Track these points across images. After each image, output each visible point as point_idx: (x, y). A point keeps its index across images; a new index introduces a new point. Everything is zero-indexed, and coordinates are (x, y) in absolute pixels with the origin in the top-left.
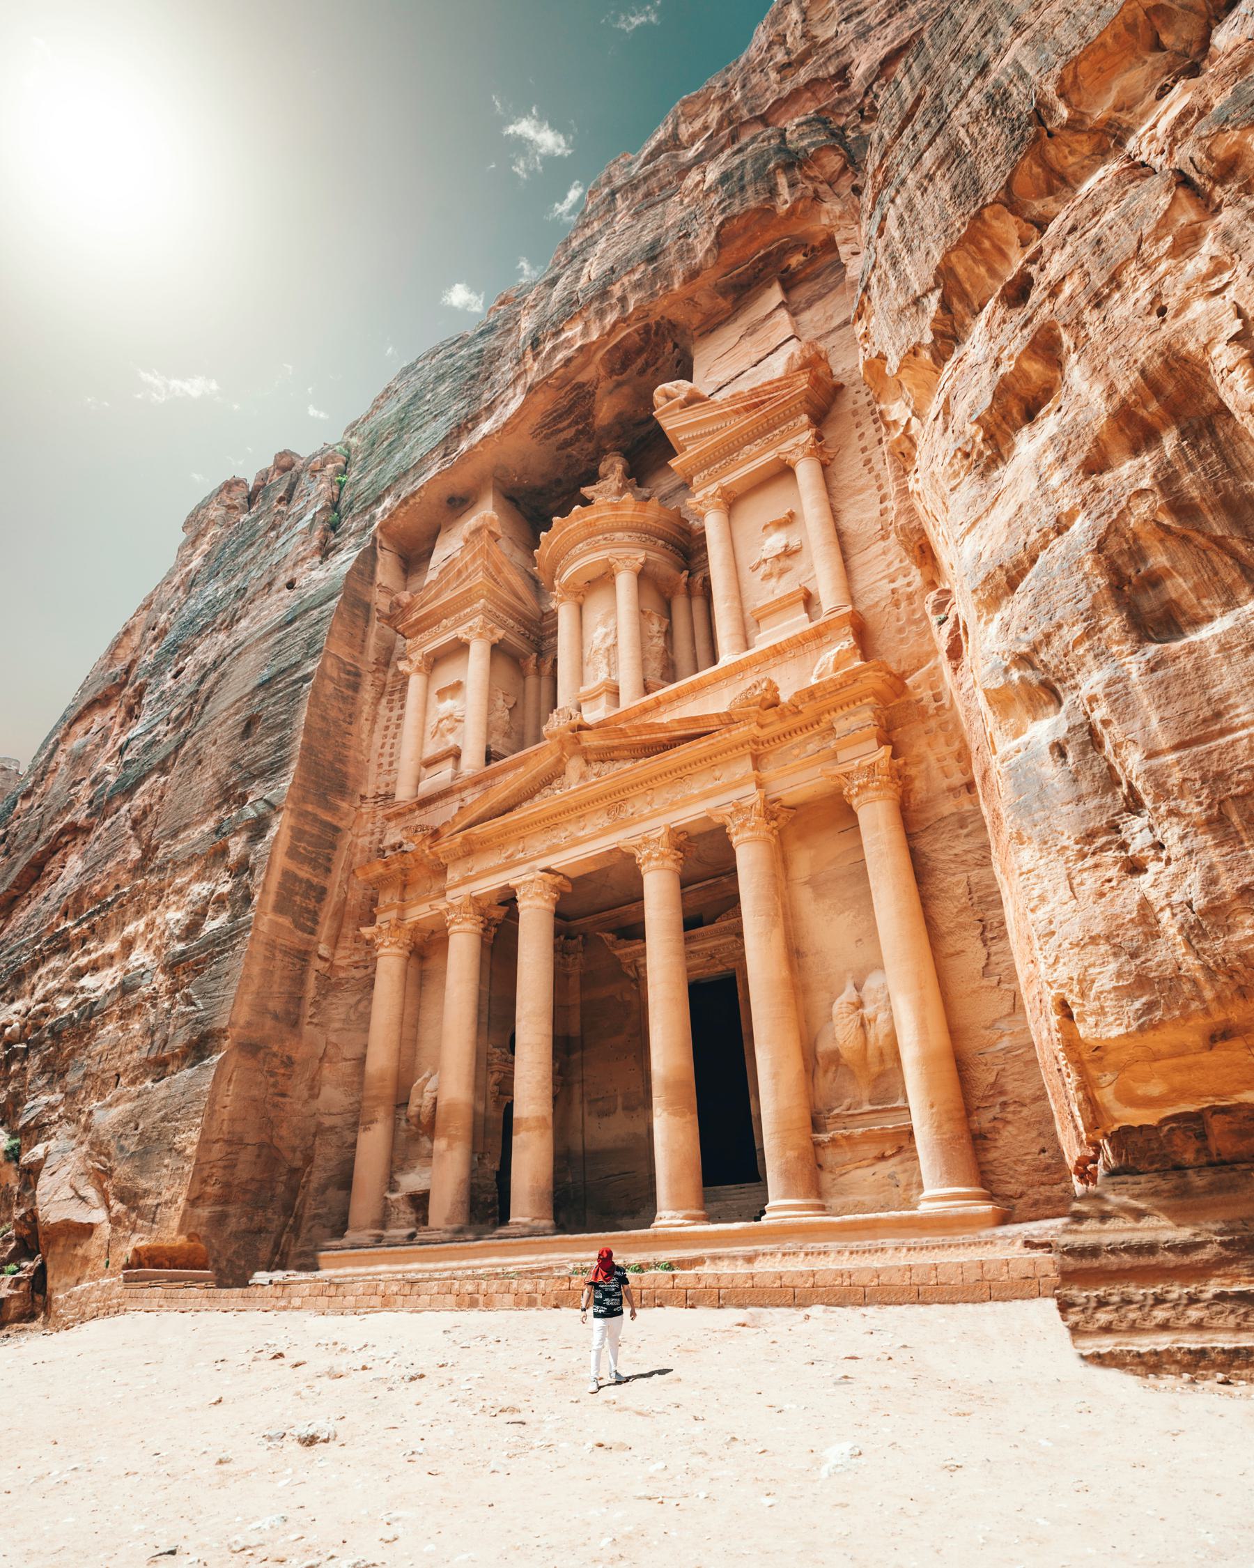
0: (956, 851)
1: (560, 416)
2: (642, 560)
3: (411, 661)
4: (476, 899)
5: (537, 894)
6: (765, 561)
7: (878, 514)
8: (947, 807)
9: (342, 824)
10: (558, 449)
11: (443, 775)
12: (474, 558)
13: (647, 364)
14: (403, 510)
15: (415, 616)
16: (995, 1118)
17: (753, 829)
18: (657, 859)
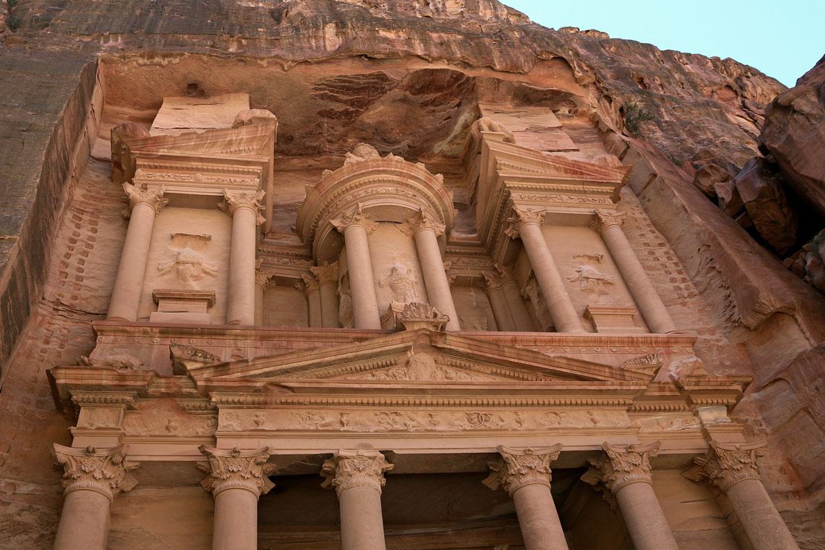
1: (348, 89)
4: (273, 459)
10: (320, 113)
11: (198, 315)
12: (251, 141)
13: (433, 102)
14: (141, 61)
15: (162, 152)
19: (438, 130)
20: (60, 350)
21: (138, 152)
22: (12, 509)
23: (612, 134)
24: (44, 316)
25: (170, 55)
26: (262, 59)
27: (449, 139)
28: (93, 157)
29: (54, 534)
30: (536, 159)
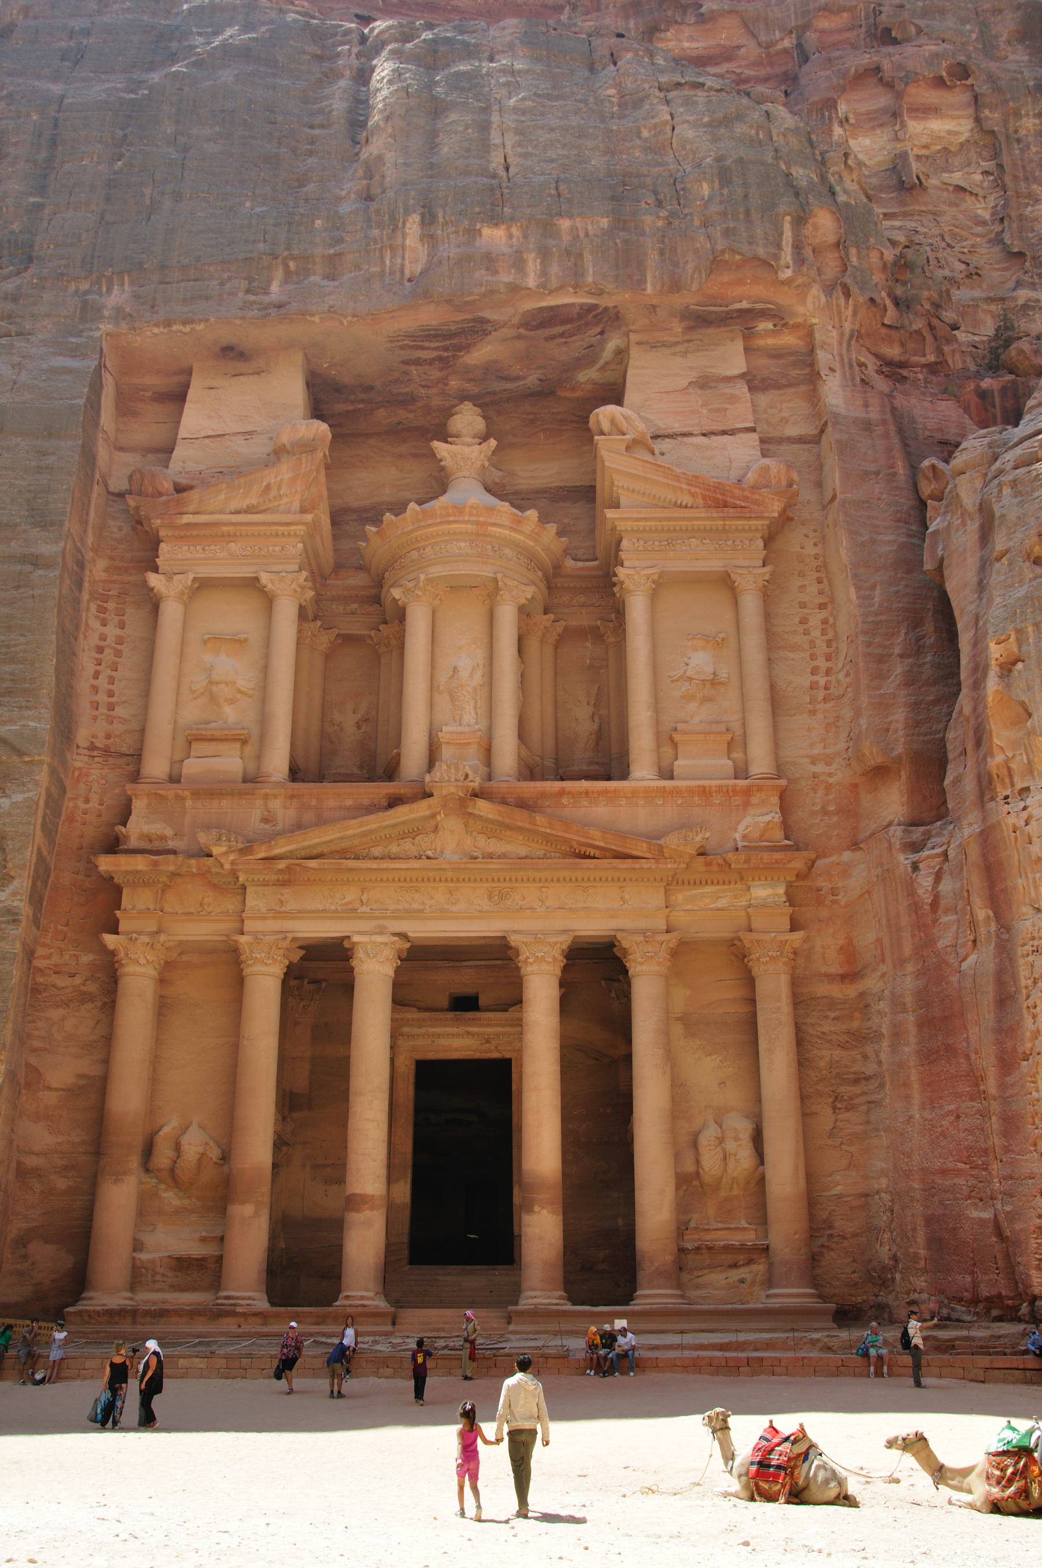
0: (826, 1029)
1: (436, 336)
2: (529, 597)
3: (170, 579)
4: (294, 939)
5: (388, 959)
6: (690, 679)
7: (807, 684)
8: (822, 989)
9: (68, 783)
10: (403, 362)
13: (562, 335)
14: (156, 330)
15: (186, 519)
16: (822, 1246)
17: (659, 964)
18: (549, 963)
19: (579, 359)
20: (100, 807)
21: (159, 521)
22: (78, 980)
23: (821, 382)
24: (80, 769)
25: (192, 322)
26: (312, 315)
27: (598, 366)
28: (113, 494)
29: (114, 1002)
30: (665, 481)
